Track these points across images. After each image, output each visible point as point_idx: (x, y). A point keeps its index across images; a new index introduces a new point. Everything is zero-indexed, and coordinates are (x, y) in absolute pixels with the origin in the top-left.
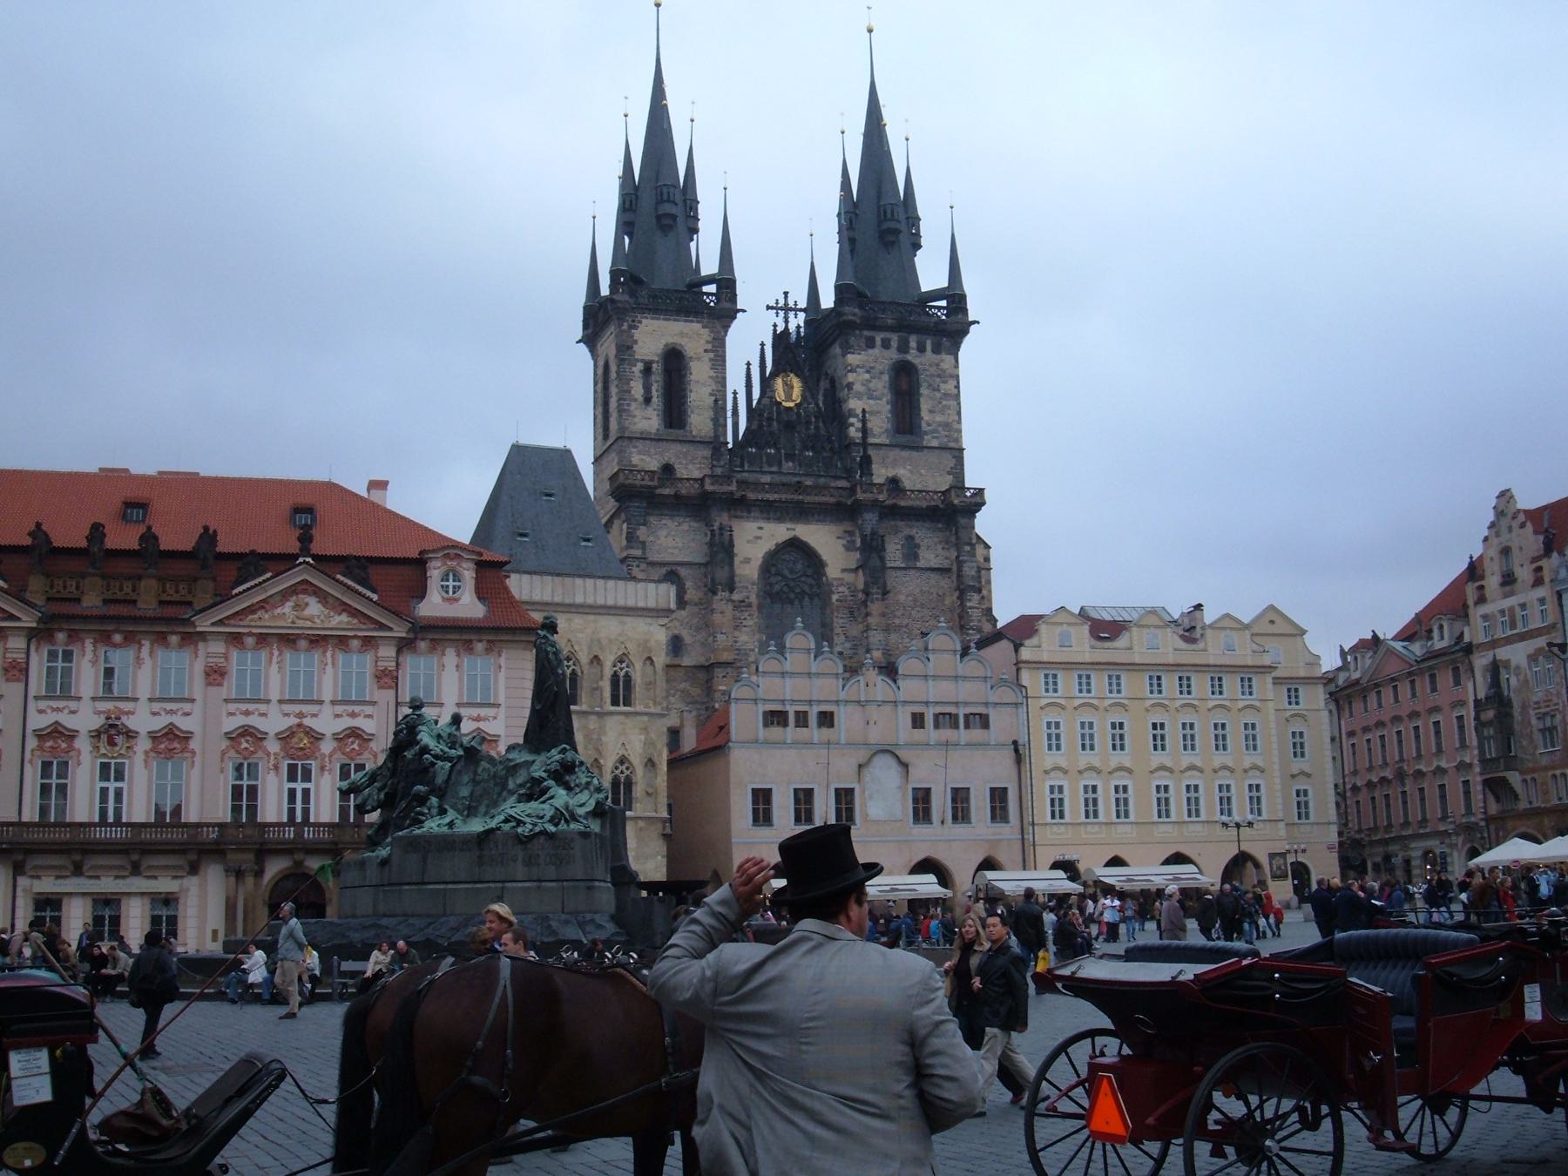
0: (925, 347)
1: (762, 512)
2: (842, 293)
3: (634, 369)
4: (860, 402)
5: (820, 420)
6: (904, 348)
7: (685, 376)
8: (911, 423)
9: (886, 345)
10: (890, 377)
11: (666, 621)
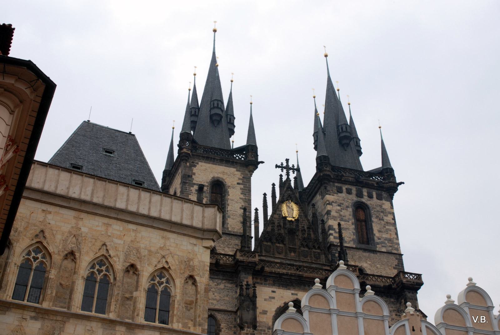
0: (373, 196)
2: (321, 161)
3: (192, 188)
4: (335, 222)
5: (311, 230)
6: (360, 195)
7: (225, 196)
8: (368, 238)
9: (349, 192)
10: (353, 210)
11: (211, 244)
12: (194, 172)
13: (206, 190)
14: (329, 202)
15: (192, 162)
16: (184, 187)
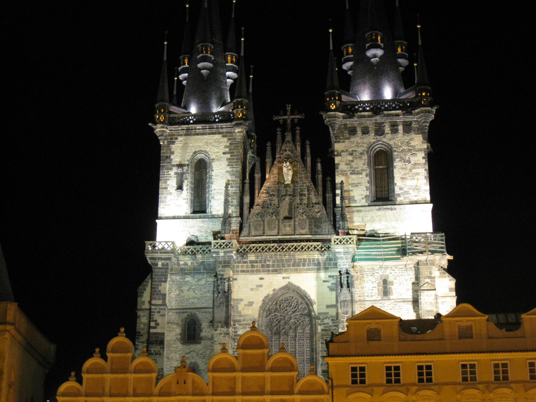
1: (263, 266)
5: (313, 193)
9: (365, 131)
10: (369, 158)
12: (173, 150)
13: (187, 170)
14: (337, 153)
15: (171, 139)
16: (162, 172)
